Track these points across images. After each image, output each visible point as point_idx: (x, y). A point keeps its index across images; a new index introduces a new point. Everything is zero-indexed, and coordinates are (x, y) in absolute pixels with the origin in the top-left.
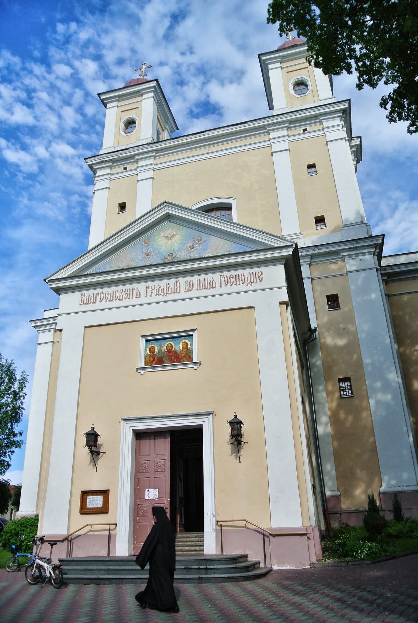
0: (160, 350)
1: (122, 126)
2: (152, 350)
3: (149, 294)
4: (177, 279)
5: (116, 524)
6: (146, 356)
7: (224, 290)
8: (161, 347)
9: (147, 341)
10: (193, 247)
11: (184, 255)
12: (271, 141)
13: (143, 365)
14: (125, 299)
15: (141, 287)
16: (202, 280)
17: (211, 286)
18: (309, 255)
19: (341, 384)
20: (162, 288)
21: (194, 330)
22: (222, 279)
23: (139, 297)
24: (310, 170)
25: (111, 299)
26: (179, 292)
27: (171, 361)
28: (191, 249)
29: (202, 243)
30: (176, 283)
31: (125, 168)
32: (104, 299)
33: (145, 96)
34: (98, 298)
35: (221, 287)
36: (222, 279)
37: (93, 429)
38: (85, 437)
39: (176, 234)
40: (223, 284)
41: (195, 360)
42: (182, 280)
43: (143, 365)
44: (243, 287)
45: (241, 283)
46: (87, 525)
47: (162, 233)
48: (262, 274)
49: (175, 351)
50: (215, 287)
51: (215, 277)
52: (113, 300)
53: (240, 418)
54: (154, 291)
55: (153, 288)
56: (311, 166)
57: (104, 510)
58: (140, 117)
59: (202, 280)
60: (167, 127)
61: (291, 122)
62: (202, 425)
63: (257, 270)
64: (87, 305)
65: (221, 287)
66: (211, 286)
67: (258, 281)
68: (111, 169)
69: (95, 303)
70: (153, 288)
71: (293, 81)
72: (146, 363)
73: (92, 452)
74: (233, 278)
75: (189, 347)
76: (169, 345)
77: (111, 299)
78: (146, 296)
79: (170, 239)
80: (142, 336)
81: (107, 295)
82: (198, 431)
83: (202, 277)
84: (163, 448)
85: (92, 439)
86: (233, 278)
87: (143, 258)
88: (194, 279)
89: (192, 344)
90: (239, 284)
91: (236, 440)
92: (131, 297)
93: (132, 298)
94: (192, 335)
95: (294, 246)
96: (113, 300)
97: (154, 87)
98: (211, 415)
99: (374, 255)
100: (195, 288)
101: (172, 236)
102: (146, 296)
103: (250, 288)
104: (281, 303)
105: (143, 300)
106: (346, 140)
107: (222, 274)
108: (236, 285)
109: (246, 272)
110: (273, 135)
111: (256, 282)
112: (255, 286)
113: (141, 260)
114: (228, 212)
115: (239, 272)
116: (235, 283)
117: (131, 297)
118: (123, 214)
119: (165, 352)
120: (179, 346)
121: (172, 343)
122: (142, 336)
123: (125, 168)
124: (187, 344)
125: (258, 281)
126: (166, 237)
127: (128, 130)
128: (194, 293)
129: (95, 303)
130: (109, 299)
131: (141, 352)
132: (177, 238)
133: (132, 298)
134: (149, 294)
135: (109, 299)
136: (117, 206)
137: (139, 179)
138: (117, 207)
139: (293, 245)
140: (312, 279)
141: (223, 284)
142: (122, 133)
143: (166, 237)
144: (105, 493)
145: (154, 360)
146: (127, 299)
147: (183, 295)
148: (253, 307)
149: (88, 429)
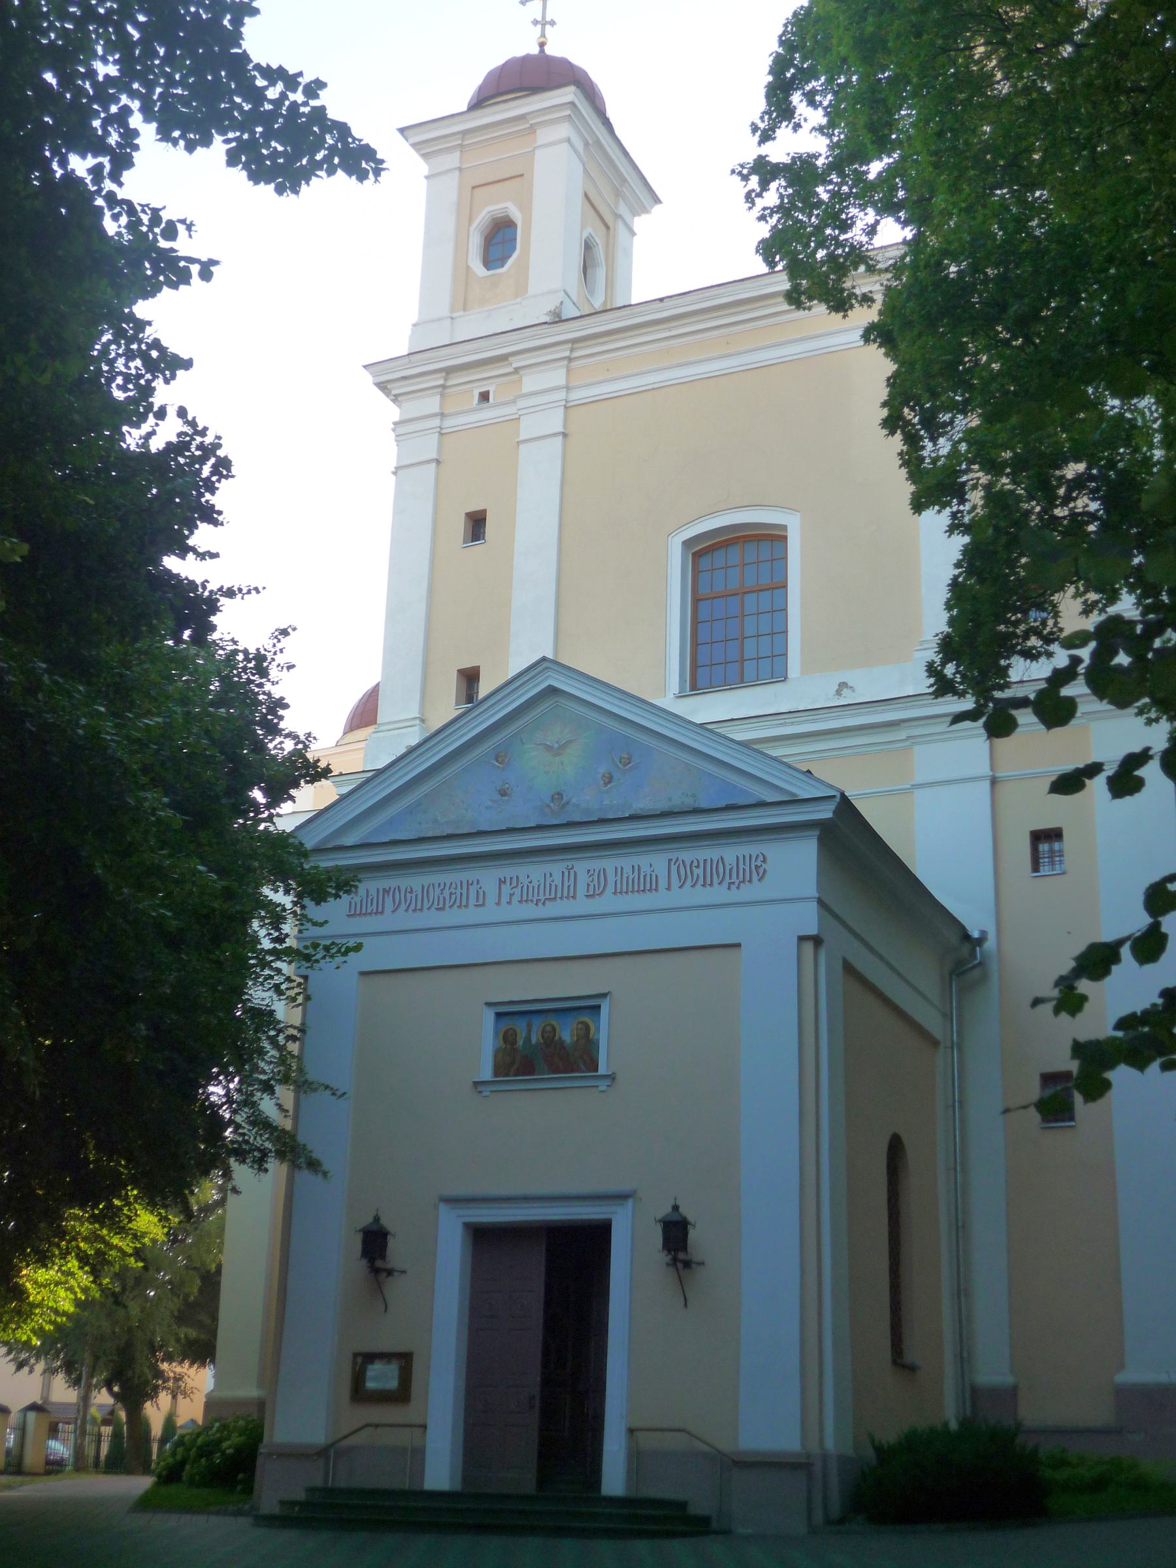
0: (528, 1039)
1: (475, 242)
2: (508, 1038)
3: (505, 899)
4: (570, 864)
5: (424, 1427)
6: (497, 1053)
8: (529, 1031)
10: (609, 779)
11: (587, 801)
14: (450, 907)
15: (488, 877)
16: (628, 870)
17: (648, 887)
20: (535, 884)
22: (674, 868)
23: (483, 905)
25: (419, 907)
26: (574, 897)
28: (606, 784)
30: (566, 874)
31: (485, 397)
32: (403, 907)
34: (389, 901)
35: (669, 889)
36: (674, 868)
37: (377, 1219)
39: (570, 742)
41: (602, 1070)
42: (583, 867)
43: (487, 1074)
44: (718, 893)
45: (716, 881)
46: (367, 1425)
48: (764, 861)
51: (656, 862)
55: (514, 884)
57: (402, 1395)
58: (526, 206)
59: (628, 870)
64: (363, 919)
65: (669, 889)
66: (648, 887)
67: (755, 877)
69: (382, 913)
70: (514, 884)
72: (497, 1071)
73: (375, 1271)
74: (698, 867)
76: (548, 1028)
77: (419, 907)
78: (498, 904)
79: (558, 754)
80: (488, 1004)
81: (409, 895)
82: (600, 1233)
83: (627, 862)
84: (533, 1268)
85: (374, 1241)
86: (698, 867)
88: (608, 864)
89: (598, 1029)
90: (711, 884)
92: (464, 903)
93: (467, 906)
94: (599, 1007)
95: (838, 799)
96: (421, 910)
98: (630, 1202)
100: (610, 888)
101: (563, 747)
102: (498, 904)
103: (735, 895)
104: (802, 939)
105: (490, 912)
108: (704, 885)
109: (730, 853)
111: (750, 881)
112: (747, 892)
113: (487, 808)
116: (701, 881)
117: (464, 903)
118: (478, 549)
120: (567, 1034)
121: (554, 1023)
122: (488, 1004)
123: (485, 397)
124: (587, 1028)
125: (755, 877)
126: (549, 748)
128: (608, 902)
129: (382, 913)
130: (412, 907)
133: (467, 906)
135: (412, 907)
137: (522, 438)
138: (458, 526)
139: (834, 797)
140: (994, 781)
143: (549, 748)
144: (405, 1360)
145: (513, 1063)
146: (455, 907)
147: (581, 905)
148: (739, 945)
149: (367, 1220)
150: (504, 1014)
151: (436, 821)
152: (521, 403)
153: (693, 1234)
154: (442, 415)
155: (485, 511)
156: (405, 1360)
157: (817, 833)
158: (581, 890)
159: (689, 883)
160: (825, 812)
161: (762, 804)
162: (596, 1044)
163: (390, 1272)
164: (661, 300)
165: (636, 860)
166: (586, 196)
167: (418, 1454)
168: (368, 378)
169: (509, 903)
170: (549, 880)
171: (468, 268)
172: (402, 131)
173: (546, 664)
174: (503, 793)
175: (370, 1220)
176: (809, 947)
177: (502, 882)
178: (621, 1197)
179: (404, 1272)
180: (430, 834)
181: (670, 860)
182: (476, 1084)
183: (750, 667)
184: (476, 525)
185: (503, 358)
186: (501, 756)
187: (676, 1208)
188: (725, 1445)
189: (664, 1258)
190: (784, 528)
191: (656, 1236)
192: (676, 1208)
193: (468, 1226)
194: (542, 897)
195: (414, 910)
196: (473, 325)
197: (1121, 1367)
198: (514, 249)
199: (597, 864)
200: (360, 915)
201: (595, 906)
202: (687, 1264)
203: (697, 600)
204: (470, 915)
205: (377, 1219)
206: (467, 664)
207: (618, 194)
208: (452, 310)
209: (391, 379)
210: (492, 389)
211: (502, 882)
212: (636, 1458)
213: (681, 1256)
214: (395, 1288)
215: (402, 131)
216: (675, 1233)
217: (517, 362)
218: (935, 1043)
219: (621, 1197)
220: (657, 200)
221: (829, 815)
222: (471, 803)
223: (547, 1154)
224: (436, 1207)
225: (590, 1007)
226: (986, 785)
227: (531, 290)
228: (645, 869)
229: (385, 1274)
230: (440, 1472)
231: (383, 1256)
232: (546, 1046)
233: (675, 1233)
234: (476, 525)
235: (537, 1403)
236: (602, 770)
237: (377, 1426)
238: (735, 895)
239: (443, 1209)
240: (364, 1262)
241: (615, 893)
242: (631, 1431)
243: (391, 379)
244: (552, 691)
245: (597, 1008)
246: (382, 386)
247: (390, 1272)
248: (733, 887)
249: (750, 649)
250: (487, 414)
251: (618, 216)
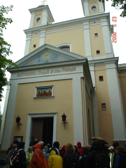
0: (42, 92)
1: (36, 20)
2: (39, 92)
6: (37, 94)
7: (63, 73)
8: (42, 91)
9: (38, 89)
10: (54, 59)
12: (84, 26)
13: (36, 96)
15: (37, 72)
16: (56, 70)
18: (94, 63)
19: (103, 106)
24: (96, 35)
27: (45, 96)
31: (36, 34)
33: (43, 10)
34: (23, 75)
35: (62, 72)
37: (19, 116)
38: (16, 119)
41: (52, 96)
43: (36, 96)
44: (69, 72)
47: (44, 54)
48: (75, 68)
49: (46, 92)
51: (60, 69)
53: (65, 115)
54: (41, 73)
56: (96, 34)
58: (42, 17)
60: (51, 20)
61: (90, 19)
62: (53, 117)
63: (74, 67)
65: (62, 72)
67: (74, 70)
68: (32, 34)
71: (91, 6)
73: (18, 124)
82: (52, 119)
85: (18, 120)
89: (52, 90)
91: (64, 122)
97: (47, 7)
98: (57, 114)
99: (115, 64)
100: (54, 72)
103: (71, 72)
104: (81, 78)
106: (108, 26)
110: (84, 24)
111: (74, 71)
112: (73, 72)
114: (68, 48)
115: (68, 67)
119: (43, 93)
120: (47, 91)
124: (50, 90)
125: (74, 70)
126: (46, 55)
127: (38, 21)
131: (35, 92)
132: (49, 56)
136: (33, 45)
138: (33, 46)
140: (95, 71)
142: (36, 22)
143: (46, 55)
144: (22, 137)
145: (39, 95)
147: (50, 74)
148: (72, 79)
150: (38, 89)
153: (66, 118)
154: (32, 35)
156: (22, 137)
157: (83, 64)
158: (50, 72)
160: (85, 61)
162: (51, 92)
165: (57, 69)
166: (48, 18)
168: (23, 32)
171: (35, 22)
172: (29, 10)
176: (82, 79)
177: (39, 72)
178: (55, 113)
179: (22, 124)
182: (34, 98)
190: (69, 46)
191: (61, 118)
197: (114, 139)
199: (52, 69)
207: (51, 19)
209: (26, 32)
210: (37, 33)
211: (39, 72)
214: (21, 127)
215: (29, 10)
216: (64, 117)
217: (40, 30)
219: (55, 113)
220: (54, 21)
221: (85, 61)
222: (35, 62)
223: (44, 108)
224: (27, 115)
225: (51, 87)
226: (94, 71)
228: (59, 69)
229: (19, 125)
231: (19, 122)
232: (44, 93)
233: (64, 117)
236: (53, 58)
239: (28, 115)
240: (16, 123)
243: (26, 32)
244: (46, 49)
245: (52, 88)
246: (25, 33)
247: (20, 125)
251: (50, 21)
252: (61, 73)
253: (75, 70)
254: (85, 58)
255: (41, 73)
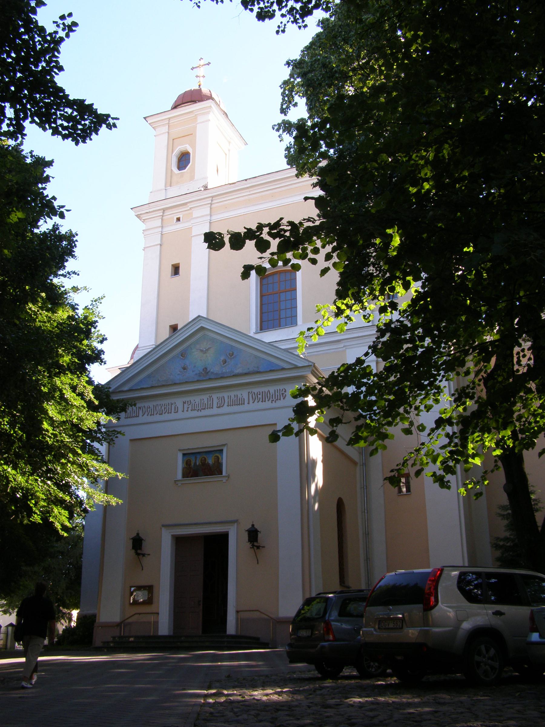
0: (195, 463)
1: (174, 160)
2: (187, 463)
3: (186, 409)
5: (158, 614)
6: (184, 469)
8: (196, 460)
9: (184, 455)
10: (225, 362)
11: (216, 369)
15: (179, 402)
16: (233, 397)
20: (197, 403)
21: (224, 445)
22: (250, 395)
23: (177, 412)
26: (212, 408)
28: (224, 364)
29: (233, 358)
31: (178, 219)
32: (146, 414)
35: (249, 403)
36: (250, 395)
37: (138, 534)
38: (131, 541)
40: (251, 401)
41: (224, 473)
44: (268, 404)
45: (267, 400)
48: (285, 391)
49: (208, 464)
50: (244, 404)
51: (243, 393)
52: (153, 415)
54: (190, 406)
57: (149, 602)
59: (233, 397)
65: (249, 403)
67: (282, 398)
69: (138, 416)
72: (184, 476)
75: (220, 460)
78: (183, 411)
79: (205, 353)
80: (180, 450)
82: (224, 538)
85: (137, 543)
87: (180, 372)
88: (226, 395)
89: (222, 458)
90: (265, 401)
93: (171, 413)
94: (222, 450)
96: (153, 415)
98: (236, 524)
100: (226, 404)
101: (207, 350)
102: (183, 411)
105: (180, 415)
107: (250, 390)
108: (262, 402)
109: (272, 389)
111: (280, 399)
115: (264, 389)
116: (261, 400)
118: (177, 278)
120: (210, 461)
122: (180, 450)
123: (178, 219)
124: (218, 457)
125: (282, 398)
126: (202, 351)
128: (225, 409)
129: (138, 416)
130: (150, 414)
133: (171, 413)
134: (186, 409)
135: (150, 414)
138: (169, 270)
141: (251, 401)
144: (149, 589)
146: (166, 414)
147: (215, 411)
149: (134, 535)
151: (159, 380)
152: (193, 221)
153: (260, 535)
155: (179, 264)
156: (149, 589)
158: (215, 405)
159: (256, 401)
161: (283, 369)
163: (144, 555)
164: (246, 180)
165: (236, 393)
167: (156, 623)
168: (133, 213)
169: (187, 411)
170: (202, 401)
171: (172, 170)
172: (145, 118)
173: (200, 318)
174: (184, 369)
175: (136, 535)
177: (184, 403)
179: (149, 555)
180: (156, 385)
181: (249, 392)
182: (176, 481)
183: (283, 321)
184: (176, 270)
185: (186, 204)
186: (183, 355)
187: (253, 525)
188: (273, 616)
189: (249, 545)
192: (253, 525)
193: (172, 535)
194: (200, 408)
195: (151, 415)
196: (173, 191)
198: (189, 162)
199: (220, 395)
200: (130, 417)
201: (220, 411)
202: (258, 547)
203: (262, 296)
204: (173, 416)
205: (138, 534)
206: (173, 323)
208: (166, 187)
209: (141, 213)
210: (181, 216)
211: (184, 403)
212: (240, 622)
213: (255, 544)
214: (146, 561)
215: (145, 118)
216: (253, 535)
217: (190, 206)
218: (355, 463)
223: (204, 508)
224: (161, 528)
227: (196, 178)
228: (239, 396)
230: (164, 627)
231: (141, 549)
232: (202, 465)
233: (253, 535)
234: (176, 270)
235: (201, 603)
236: (222, 358)
237: (140, 614)
238: (274, 405)
239: (163, 529)
240: (133, 551)
241: (228, 406)
242: (238, 612)
243: (141, 213)
245: (221, 451)
247: (144, 555)
248: (273, 402)
249: (283, 315)
250: (180, 226)
252: (246, 407)
253: (284, 399)
254: (310, 364)
255: (190, 406)
